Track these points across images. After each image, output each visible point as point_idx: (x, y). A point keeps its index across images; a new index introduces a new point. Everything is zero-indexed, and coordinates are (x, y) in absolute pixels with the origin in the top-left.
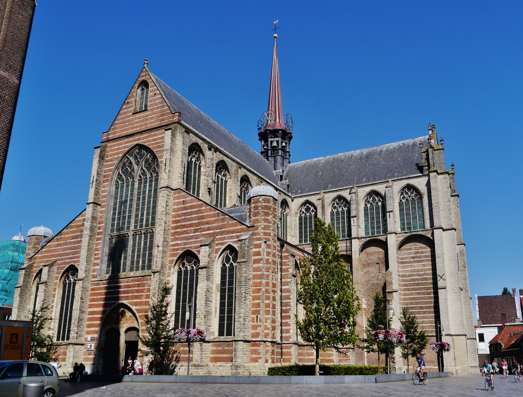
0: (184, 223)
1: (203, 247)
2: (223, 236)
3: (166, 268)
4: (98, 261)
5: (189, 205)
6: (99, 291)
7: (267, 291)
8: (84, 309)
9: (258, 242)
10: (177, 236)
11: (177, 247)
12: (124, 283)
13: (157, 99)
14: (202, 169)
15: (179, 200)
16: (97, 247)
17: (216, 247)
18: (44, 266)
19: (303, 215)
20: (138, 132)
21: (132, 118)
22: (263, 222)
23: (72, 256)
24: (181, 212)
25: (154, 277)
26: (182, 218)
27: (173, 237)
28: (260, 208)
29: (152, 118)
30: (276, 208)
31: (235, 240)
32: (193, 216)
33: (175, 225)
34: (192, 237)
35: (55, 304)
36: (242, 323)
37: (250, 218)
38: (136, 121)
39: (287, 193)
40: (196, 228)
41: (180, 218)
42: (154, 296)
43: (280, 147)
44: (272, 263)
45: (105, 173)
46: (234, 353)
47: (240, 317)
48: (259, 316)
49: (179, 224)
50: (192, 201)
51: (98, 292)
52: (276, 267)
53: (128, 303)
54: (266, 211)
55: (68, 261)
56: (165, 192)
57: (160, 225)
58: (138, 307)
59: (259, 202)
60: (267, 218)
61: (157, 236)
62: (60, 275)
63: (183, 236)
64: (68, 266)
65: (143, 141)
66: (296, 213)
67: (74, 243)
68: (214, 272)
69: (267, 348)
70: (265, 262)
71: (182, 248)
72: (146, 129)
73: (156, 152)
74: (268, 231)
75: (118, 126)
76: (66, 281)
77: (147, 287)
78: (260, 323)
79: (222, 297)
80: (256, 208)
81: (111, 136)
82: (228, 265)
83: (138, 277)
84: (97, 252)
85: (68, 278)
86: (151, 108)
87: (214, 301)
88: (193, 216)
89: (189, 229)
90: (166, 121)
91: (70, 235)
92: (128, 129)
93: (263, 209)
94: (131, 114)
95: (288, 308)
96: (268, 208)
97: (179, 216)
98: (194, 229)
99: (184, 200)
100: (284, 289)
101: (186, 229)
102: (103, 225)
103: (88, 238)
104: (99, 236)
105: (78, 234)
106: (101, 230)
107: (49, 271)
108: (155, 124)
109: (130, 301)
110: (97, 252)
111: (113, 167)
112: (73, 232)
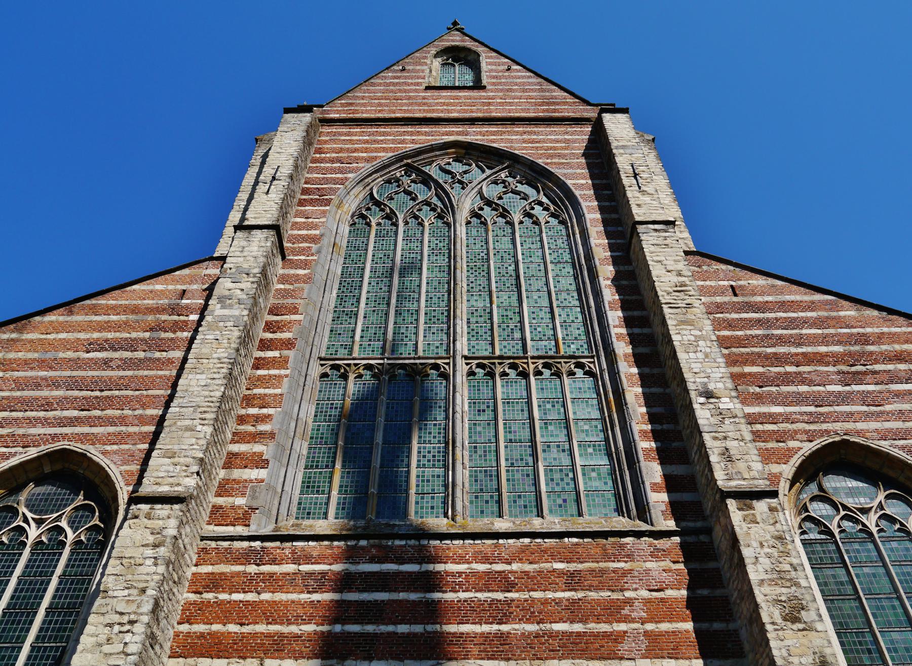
6: (266, 596)
12: (461, 560)
23: (75, 413)
24: (735, 316)
51: (251, 597)
71: (806, 432)
77: (645, 594)
88: (804, 331)
91: (82, 336)
97: (731, 325)
99: (733, 283)
101: (791, 369)
105: (134, 335)
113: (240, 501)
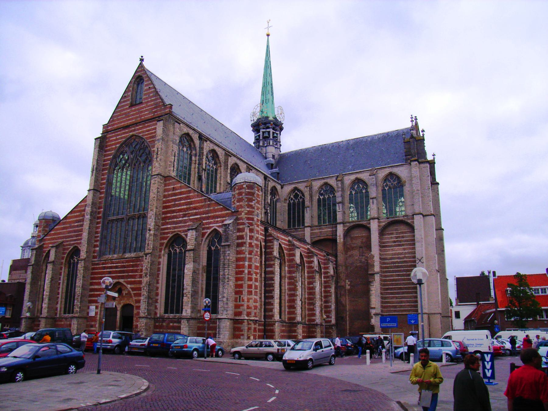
0: (173, 209)
1: (191, 231)
2: (210, 221)
3: (157, 250)
4: (98, 243)
5: (179, 191)
7: (249, 273)
8: (86, 287)
9: (241, 227)
10: (168, 221)
11: (167, 231)
13: (151, 93)
14: (193, 158)
15: (170, 187)
16: (97, 230)
17: (203, 231)
18: (52, 247)
19: (292, 202)
20: (133, 123)
21: (128, 111)
22: (246, 207)
23: (75, 238)
24: (171, 198)
25: (146, 259)
26: (172, 203)
27: (164, 221)
28: (243, 194)
29: (146, 110)
30: (260, 194)
31: (220, 224)
32: (182, 202)
33: (166, 210)
34: (180, 222)
35: (61, 281)
36: (225, 302)
37: (234, 204)
38: (132, 113)
39: (277, 181)
40: (184, 213)
41: (170, 204)
42: (146, 276)
43: (271, 137)
44: (255, 247)
45: (104, 162)
46: (217, 330)
47: (224, 297)
48: (242, 296)
49: (169, 209)
50: (181, 188)
52: (259, 250)
53: (124, 281)
54: (250, 197)
55: (72, 242)
56: (156, 179)
57: (151, 210)
58: (133, 286)
59: (243, 188)
60: (250, 203)
61: (148, 220)
62: (66, 256)
63: (173, 220)
64: (72, 247)
65: (137, 132)
66: (285, 200)
67: (77, 226)
68: (201, 254)
69: (250, 326)
70: (248, 246)
72: (141, 121)
73: (149, 142)
74: (251, 216)
75: (116, 118)
76: (71, 261)
78: (243, 303)
79: (208, 279)
80: (240, 194)
81: (110, 128)
82: (213, 248)
83: (132, 258)
84: (97, 235)
85: (73, 258)
86: (146, 101)
87: (200, 281)
88: (182, 202)
89: (178, 214)
90: (158, 113)
91: (74, 219)
92: (124, 121)
93: (246, 195)
94: (128, 107)
95: (271, 288)
96: (253, 194)
98: (182, 214)
100: (268, 271)
101: (175, 214)
102: (102, 210)
103: (88, 222)
104: (99, 220)
106: (100, 215)
107: (56, 251)
108: (149, 116)
109: (125, 280)
110: (97, 235)
111: (111, 157)
112: (76, 216)
113: (96, 254)
